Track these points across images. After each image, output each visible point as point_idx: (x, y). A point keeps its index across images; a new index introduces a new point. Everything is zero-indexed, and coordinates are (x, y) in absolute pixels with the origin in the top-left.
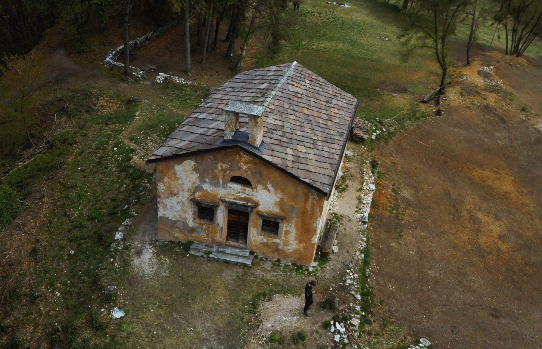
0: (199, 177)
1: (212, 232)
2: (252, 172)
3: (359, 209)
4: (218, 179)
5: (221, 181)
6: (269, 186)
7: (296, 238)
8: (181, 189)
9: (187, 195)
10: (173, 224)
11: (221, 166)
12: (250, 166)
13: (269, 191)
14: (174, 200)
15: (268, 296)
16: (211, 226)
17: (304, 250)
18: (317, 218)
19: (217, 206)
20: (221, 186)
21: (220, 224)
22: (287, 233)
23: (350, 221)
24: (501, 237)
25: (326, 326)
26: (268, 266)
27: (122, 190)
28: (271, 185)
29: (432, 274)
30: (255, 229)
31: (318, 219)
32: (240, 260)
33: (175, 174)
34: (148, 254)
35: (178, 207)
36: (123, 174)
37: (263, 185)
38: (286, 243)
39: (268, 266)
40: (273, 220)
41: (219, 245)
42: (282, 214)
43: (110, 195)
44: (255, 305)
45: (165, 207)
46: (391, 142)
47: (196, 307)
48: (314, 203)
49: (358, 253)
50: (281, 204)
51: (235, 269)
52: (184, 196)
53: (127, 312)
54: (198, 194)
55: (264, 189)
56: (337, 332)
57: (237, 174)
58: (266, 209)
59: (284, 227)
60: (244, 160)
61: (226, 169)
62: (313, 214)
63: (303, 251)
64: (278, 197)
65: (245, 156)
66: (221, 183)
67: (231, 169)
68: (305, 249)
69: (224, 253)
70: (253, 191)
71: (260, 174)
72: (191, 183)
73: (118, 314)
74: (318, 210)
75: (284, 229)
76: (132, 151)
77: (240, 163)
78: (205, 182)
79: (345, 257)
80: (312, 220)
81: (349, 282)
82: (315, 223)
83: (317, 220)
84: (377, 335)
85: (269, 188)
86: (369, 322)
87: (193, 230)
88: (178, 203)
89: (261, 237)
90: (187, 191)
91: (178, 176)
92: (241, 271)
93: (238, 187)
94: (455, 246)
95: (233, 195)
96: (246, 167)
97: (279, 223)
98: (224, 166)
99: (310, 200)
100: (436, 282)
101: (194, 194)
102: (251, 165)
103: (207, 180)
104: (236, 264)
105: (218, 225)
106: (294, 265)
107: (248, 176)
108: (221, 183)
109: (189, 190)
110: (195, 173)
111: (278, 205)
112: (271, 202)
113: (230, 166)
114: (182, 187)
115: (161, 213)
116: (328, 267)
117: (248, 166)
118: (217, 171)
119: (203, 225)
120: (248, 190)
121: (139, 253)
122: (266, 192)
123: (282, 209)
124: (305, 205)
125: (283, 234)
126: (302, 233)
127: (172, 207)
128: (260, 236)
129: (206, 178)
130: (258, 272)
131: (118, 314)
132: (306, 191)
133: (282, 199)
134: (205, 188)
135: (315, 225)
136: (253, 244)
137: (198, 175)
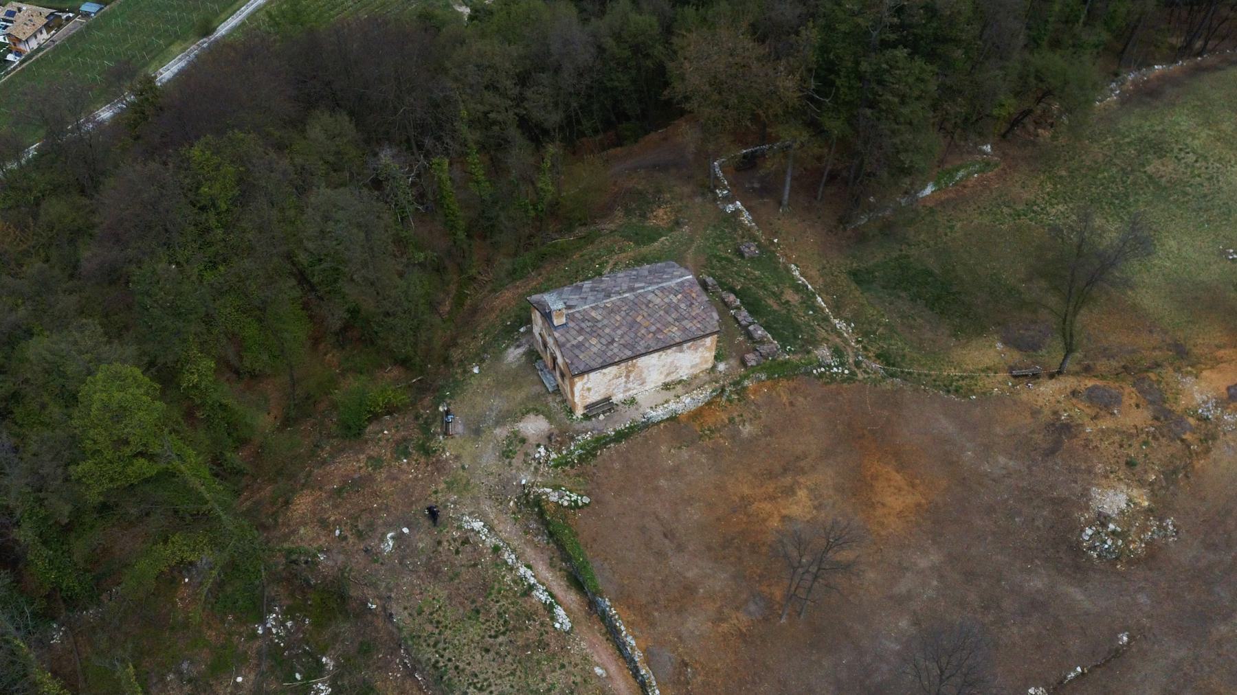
23: (637, 409)
29: (662, 482)
32: (548, 385)
44: (528, 412)
47: (506, 393)
53: (480, 372)
73: (476, 370)
81: (580, 437)
84: (568, 475)
86: (572, 467)
92: (544, 391)
116: (585, 423)
121: (518, 346)
130: (550, 399)
131: (476, 370)
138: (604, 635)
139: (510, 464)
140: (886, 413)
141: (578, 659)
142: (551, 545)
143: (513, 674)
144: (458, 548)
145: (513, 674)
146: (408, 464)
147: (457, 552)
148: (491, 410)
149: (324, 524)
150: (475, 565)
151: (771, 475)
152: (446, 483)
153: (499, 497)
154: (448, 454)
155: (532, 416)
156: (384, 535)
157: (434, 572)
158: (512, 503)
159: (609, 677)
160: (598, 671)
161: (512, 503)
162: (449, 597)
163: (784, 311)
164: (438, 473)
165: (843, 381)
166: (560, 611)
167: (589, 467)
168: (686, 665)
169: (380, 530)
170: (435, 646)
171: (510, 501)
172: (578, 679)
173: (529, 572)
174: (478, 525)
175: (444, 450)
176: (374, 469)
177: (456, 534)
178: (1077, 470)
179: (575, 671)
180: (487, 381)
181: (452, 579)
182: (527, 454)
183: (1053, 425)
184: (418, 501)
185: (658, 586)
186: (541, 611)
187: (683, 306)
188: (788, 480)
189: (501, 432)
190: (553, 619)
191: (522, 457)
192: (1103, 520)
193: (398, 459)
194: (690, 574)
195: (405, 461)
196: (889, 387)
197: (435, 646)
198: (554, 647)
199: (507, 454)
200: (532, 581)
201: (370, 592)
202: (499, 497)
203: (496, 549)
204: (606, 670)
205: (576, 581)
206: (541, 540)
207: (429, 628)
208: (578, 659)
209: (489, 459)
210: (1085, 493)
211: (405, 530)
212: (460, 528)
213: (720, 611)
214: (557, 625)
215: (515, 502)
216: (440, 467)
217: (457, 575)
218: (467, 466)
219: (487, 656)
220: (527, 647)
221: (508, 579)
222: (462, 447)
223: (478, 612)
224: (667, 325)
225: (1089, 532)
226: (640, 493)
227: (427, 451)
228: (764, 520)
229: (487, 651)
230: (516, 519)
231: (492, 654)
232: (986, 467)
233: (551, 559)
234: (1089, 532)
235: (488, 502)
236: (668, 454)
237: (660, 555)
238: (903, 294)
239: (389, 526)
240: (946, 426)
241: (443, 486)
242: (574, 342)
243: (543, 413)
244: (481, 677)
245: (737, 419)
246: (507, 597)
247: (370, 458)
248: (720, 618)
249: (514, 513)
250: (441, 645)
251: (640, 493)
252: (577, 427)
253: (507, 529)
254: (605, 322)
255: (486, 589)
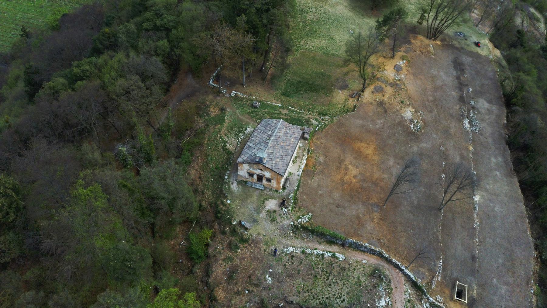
3: (298, 171)
9: (246, 171)
10: (242, 176)
15: (267, 199)
23: (295, 175)
24: (355, 177)
25: (282, 209)
26: (268, 190)
27: (225, 158)
29: (320, 192)
32: (260, 188)
34: (235, 184)
35: (244, 173)
36: (224, 152)
38: (273, 185)
39: (268, 190)
41: (255, 183)
43: (221, 160)
44: (264, 202)
45: (240, 172)
46: (324, 130)
47: (249, 201)
49: (295, 187)
50: (271, 176)
51: (259, 191)
52: (245, 171)
53: (231, 201)
54: (249, 171)
56: (284, 211)
68: (279, 187)
69: (256, 185)
73: (229, 202)
76: (227, 142)
79: (291, 188)
81: (290, 197)
84: (297, 211)
86: (295, 208)
87: (247, 178)
92: (261, 191)
93: (260, 171)
94: (333, 181)
100: (321, 195)
104: (259, 189)
106: (276, 190)
107: (262, 169)
115: (239, 173)
116: (286, 191)
120: (262, 172)
121: (232, 184)
130: (265, 192)
138: (354, 250)
139: (277, 222)
140: (343, 129)
141: (355, 264)
142: (314, 237)
143: (344, 284)
144: (292, 262)
145: (344, 284)
146: (241, 250)
147: (293, 263)
148: (251, 210)
149: (238, 293)
150: (301, 263)
151: (339, 168)
152: (264, 245)
153: (285, 236)
154: (254, 236)
155: (266, 202)
156: (265, 278)
157: (292, 276)
158: (291, 234)
159: (368, 261)
160: (364, 262)
161: (291, 234)
162: (303, 280)
163: (289, 117)
164: (258, 244)
165: (325, 127)
166: (337, 255)
167: (300, 204)
168: (379, 239)
169: (262, 278)
170: (314, 298)
171: (290, 234)
172: (362, 269)
173: (318, 251)
174: (291, 249)
175: (251, 235)
176: (231, 262)
177: (287, 258)
178: (395, 112)
179: (359, 267)
180: (237, 202)
181: (298, 273)
182: (280, 215)
183: (378, 104)
184: (263, 258)
185: (351, 223)
186: (332, 259)
187: (288, 131)
188: (343, 166)
189: (263, 215)
190: (337, 258)
191: (279, 217)
192: (411, 121)
193: (236, 252)
194: (354, 213)
195: (239, 250)
196: (336, 121)
197: (314, 298)
198: (347, 266)
199: (273, 220)
200: (321, 252)
201: (277, 301)
202: (285, 236)
203: (303, 252)
204: (365, 260)
205: (331, 242)
206: (310, 237)
207: (306, 294)
208: (355, 264)
209: (269, 226)
210: (402, 117)
211: (271, 270)
212: (286, 255)
213: (370, 217)
214: (341, 259)
215: (292, 233)
216: (256, 242)
217: (299, 271)
218: (265, 234)
219: (332, 287)
220: (339, 273)
221: (314, 258)
222: (256, 230)
223: (316, 276)
224: (290, 140)
225: (412, 126)
226: (318, 200)
227: (244, 241)
228: (351, 182)
229: (330, 285)
230: (297, 238)
231: (332, 284)
232: (377, 126)
233: (318, 241)
234: (412, 126)
235: (284, 240)
236: (314, 182)
237: (343, 214)
238: (302, 92)
239: (263, 274)
240: (359, 122)
241: (265, 247)
242: (274, 165)
243: (269, 198)
244: (336, 294)
245: (317, 158)
246: (319, 264)
247: (224, 260)
248: (372, 220)
249: (294, 236)
250: (316, 296)
251: (318, 200)
252: (285, 194)
253: (298, 243)
254: (275, 152)
255: (311, 267)
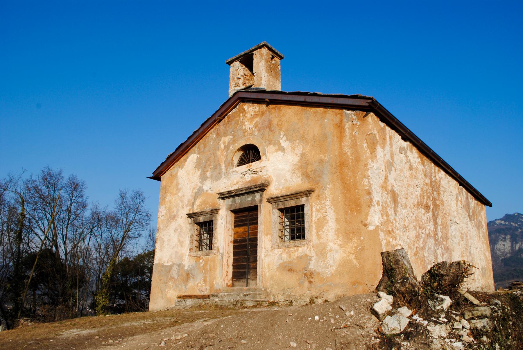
0: (200, 174)
1: (210, 270)
2: (259, 130)
4: (220, 165)
5: (223, 166)
6: (284, 143)
7: (338, 232)
8: (181, 204)
11: (224, 143)
12: (257, 122)
13: (282, 149)
14: (174, 225)
16: (210, 257)
17: (357, 258)
18: (366, 165)
19: (215, 211)
20: (223, 175)
21: (220, 248)
22: (321, 224)
28: (285, 138)
30: (269, 237)
31: (369, 166)
33: (178, 184)
37: (274, 144)
38: (322, 252)
40: (292, 203)
42: (305, 186)
48: (355, 136)
55: (277, 151)
57: (242, 143)
58: (281, 187)
59: (314, 213)
60: (248, 116)
61: (229, 143)
62: (357, 159)
63: (355, 262)
64: (297, 154)
65: (250, 109)
66: (223, 170)
67: (234, 141)
70: (261, 162)
71: (269, 126)
72: (192, 189)
74: (365, 145)
75: (314, 219)
77: (244, 123)
78: (207, 178)
80: (359, 173)
82: (364, 176)
83: (367, 170)
85: (283, 144)
88: (176, 230)
89: (278, 251)
90: (187, 205)
91: (179, 187)
95: (237, 183)
96: (251, 126)
97: (303, 206)
98: (227, 139)
99: (348, 132)
101: (193, 205)
102: (257, 119)
103: (208, 174)
105: (218, 250)
108: (223, 170)
109: (189, 201)
110: (197, 171)
111: (299, 169)
112: (288, 169)
113: (234, 136)
114: (182, 201)
117: (254, 122)
118: (219, 153)
119: (200, 259)
120: (255, 165)
122: (280, 153)
123: (306, 175)
124: (341, 148)
125: (314, 231)
126: (346, 213)
127: (169, 240)
128: (276, 251)
129: (207, 171)
132: (337, 119)
133: (303, 155)
134: (205, 188)
135: (365, 182)
136: (267, 274)
137: (199, 173)
